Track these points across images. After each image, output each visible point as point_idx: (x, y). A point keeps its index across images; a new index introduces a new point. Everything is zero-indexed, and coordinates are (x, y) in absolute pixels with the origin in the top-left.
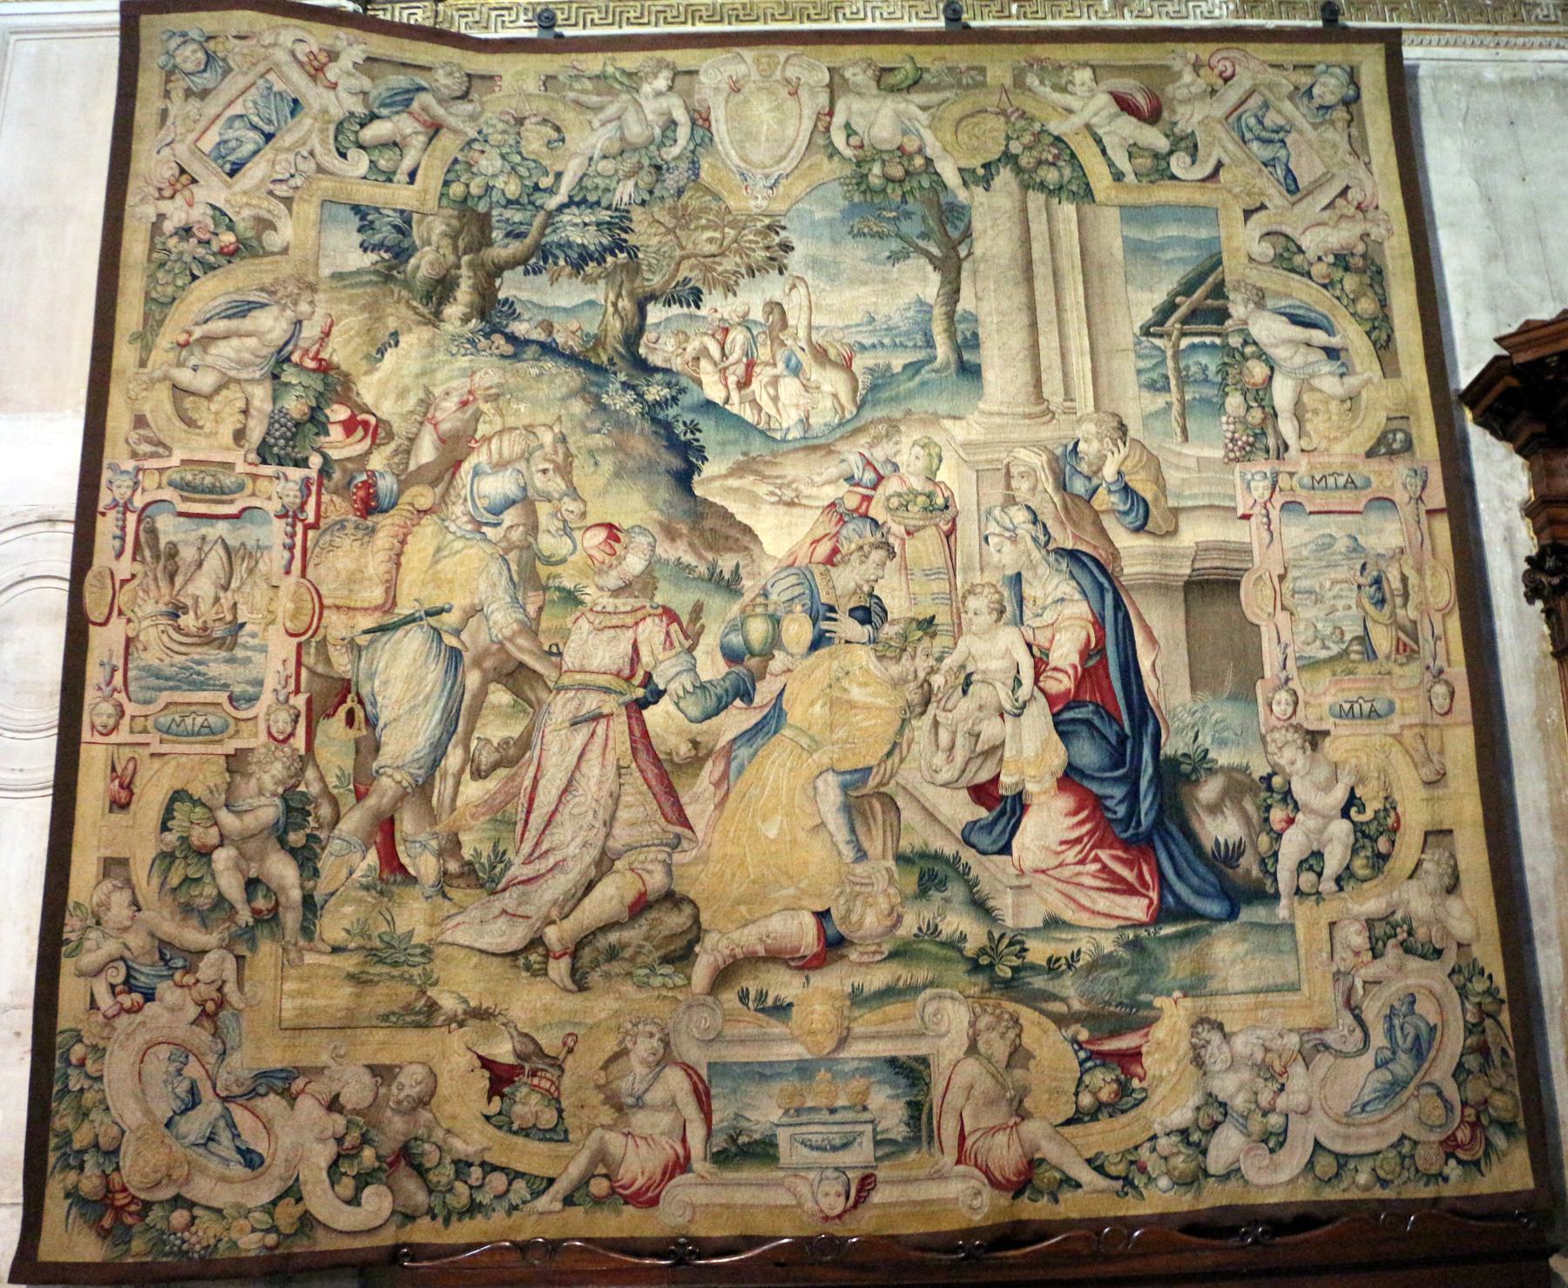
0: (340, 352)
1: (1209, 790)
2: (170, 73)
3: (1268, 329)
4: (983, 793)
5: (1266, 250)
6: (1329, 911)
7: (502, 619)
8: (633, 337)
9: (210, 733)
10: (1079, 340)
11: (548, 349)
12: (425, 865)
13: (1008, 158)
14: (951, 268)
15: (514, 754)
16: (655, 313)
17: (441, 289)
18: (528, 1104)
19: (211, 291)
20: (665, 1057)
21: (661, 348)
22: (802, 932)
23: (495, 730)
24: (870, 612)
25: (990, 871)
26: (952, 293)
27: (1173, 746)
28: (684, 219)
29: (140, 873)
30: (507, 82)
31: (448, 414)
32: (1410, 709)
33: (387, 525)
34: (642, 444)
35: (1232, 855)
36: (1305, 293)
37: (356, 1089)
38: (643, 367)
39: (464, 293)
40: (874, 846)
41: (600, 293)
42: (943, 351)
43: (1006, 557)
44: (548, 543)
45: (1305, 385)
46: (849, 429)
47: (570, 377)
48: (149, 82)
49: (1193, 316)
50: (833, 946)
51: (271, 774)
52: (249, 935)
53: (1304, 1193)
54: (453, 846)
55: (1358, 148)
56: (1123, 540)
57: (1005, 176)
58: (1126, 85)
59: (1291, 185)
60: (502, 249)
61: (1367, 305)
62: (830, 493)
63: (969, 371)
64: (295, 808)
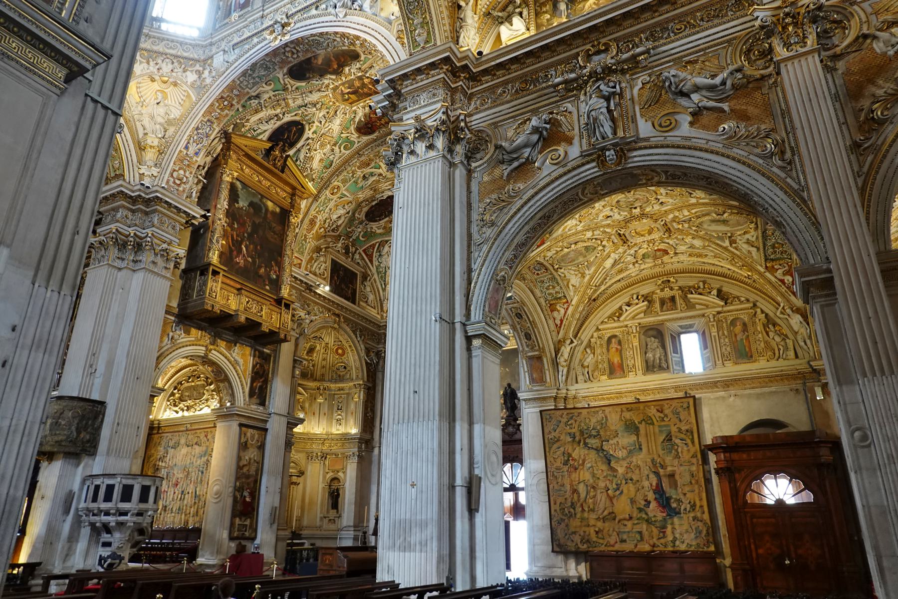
0: (570, 451)
1: (672, 501)
2: (546, 419)
3: (678, 441)
4: (646, 501)
5: (677, 430)
6: (688, 515)
7: (591, 481)
8: (602, 446)
9: (563, 496)
10: (653, 444)
11: (592, 448)
12: (586, 509)
13: (644, 420)
14: (638, 435)
15: (594, 496)
16: (604, 443)
17: (579, 442)
18: (600, 535)
19: (555, 446)
20: (614, 530)
21: (605, 448)
22: (627, 516)
23: (592, 494)
24: (631, 480)
25: (647, 510)
26: (638, 439)
27: (667, 495)
28: (606, 431)
29: (558, 510)
30: (583, 414)
31: (582, 457)
32: (697, 491)
33: (578, 471)
34: (604, 460)
35: (675, 509)
36: (683, 436)
37: (582, 534)
38: (603, 450)
39: (582, 442)
40: (634, 507)
41: (597, 441)
42: (637, 446)
43: (646, 473)
44: (595, 472)
45: (682, 449)
46: (627, 457)
47: (595, 452)
48: (544, 420)
49: (668, 440)
50: (631, 518)
51: (569, 500)
52: (569, 517)
53: (687, 549)
54: (589, 507)
55: (689, 414)
56: (660, 470)
57: (643, 422)
58: (657, 407)
59: (680, 420)
60: (586, 436)
61: (691, 437)
62: (626, 465)
63: (641, 449)
64: (572, 504)
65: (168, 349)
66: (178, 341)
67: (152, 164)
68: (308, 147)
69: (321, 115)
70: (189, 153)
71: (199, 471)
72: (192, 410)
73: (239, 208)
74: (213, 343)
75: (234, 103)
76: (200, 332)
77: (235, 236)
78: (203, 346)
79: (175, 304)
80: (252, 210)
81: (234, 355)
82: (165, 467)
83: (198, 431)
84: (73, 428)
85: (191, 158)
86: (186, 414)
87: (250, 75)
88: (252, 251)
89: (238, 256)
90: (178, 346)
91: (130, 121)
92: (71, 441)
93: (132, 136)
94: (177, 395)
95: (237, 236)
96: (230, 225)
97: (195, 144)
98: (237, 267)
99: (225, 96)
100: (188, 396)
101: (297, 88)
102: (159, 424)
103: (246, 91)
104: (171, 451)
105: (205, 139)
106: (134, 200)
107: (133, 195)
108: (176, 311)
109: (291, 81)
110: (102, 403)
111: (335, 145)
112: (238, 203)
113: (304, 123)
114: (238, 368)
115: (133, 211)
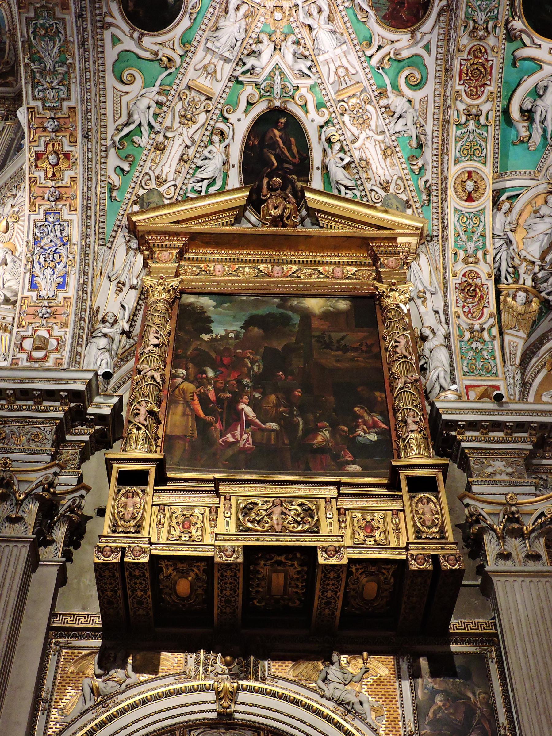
66: (120, 697)
68: (337, 146)
69: (289, 57)
70: (43, 293)
73: (213, 340)
75: (66, 148)
78: (202, 689)
80: (256, 331)
87: (42, 72)
88: (277, 406)
95: (217, 391)
97: (49, 271)
99: (42, 148)
101: (185, 42)
103: (65, 109)
105: (62, 250)
109: (159, 39)
111: (383, 94)
113: (277, 103)
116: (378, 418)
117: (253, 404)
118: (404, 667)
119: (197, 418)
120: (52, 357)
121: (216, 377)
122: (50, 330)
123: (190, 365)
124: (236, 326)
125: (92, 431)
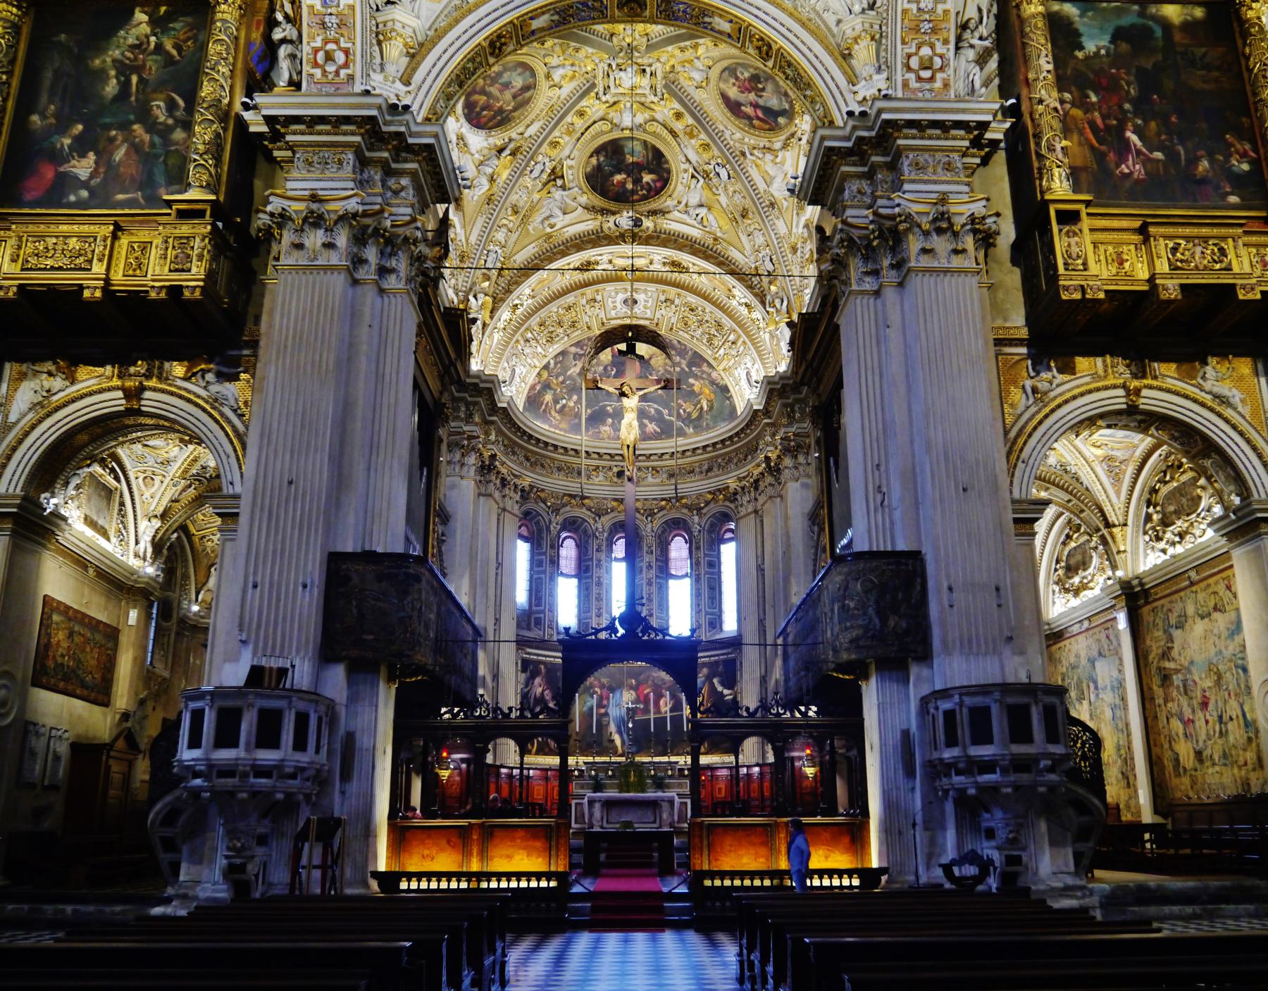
65: (1033, 416)
66: (1052, 394)
67: (872, 70)
70: (922, 5)
71: (1236, 667)
72: (1188, 537)
73: (1087, 58)
74: (1140, 374)
76: (1099, 360)
77: (1099, 121)
78: (1115, 387)
79: (1017, 321)
80: (1124, 47)
81: (1208, 386)
82: (1177, 671)
83: (1211, 581)
84: (871, 611)
85: (933, 11)
86: (1179, 549)
88: (1158, 134)
89: (1122, 159)
90: (1059, 401)
91: (810, 20)
92: (873, 637)
93: (821, 42)
94: (1155, 517)
95: (1104, 117)
96: (1081, 103)
98: (1128, 184)
100: (1175, 512)
102: (1141, 584)
104: (1177, 634)
106: (859, 151)
107: (850, 144)
108: (1024, 333)
110: (919, 553)
112: (1081, 48)
114: (1229, 413)
115: (869, 176)
116: (1248, 147)
117: (1136, 131)
118: (1260, 366)
119: (1092, 147)
120: (939, 76)
121: (1099, 101)
122: (932, 47)
123: (1073, 89)
124: (1104, 41)
125: (983, 153)
